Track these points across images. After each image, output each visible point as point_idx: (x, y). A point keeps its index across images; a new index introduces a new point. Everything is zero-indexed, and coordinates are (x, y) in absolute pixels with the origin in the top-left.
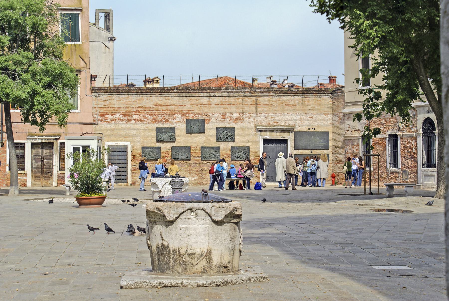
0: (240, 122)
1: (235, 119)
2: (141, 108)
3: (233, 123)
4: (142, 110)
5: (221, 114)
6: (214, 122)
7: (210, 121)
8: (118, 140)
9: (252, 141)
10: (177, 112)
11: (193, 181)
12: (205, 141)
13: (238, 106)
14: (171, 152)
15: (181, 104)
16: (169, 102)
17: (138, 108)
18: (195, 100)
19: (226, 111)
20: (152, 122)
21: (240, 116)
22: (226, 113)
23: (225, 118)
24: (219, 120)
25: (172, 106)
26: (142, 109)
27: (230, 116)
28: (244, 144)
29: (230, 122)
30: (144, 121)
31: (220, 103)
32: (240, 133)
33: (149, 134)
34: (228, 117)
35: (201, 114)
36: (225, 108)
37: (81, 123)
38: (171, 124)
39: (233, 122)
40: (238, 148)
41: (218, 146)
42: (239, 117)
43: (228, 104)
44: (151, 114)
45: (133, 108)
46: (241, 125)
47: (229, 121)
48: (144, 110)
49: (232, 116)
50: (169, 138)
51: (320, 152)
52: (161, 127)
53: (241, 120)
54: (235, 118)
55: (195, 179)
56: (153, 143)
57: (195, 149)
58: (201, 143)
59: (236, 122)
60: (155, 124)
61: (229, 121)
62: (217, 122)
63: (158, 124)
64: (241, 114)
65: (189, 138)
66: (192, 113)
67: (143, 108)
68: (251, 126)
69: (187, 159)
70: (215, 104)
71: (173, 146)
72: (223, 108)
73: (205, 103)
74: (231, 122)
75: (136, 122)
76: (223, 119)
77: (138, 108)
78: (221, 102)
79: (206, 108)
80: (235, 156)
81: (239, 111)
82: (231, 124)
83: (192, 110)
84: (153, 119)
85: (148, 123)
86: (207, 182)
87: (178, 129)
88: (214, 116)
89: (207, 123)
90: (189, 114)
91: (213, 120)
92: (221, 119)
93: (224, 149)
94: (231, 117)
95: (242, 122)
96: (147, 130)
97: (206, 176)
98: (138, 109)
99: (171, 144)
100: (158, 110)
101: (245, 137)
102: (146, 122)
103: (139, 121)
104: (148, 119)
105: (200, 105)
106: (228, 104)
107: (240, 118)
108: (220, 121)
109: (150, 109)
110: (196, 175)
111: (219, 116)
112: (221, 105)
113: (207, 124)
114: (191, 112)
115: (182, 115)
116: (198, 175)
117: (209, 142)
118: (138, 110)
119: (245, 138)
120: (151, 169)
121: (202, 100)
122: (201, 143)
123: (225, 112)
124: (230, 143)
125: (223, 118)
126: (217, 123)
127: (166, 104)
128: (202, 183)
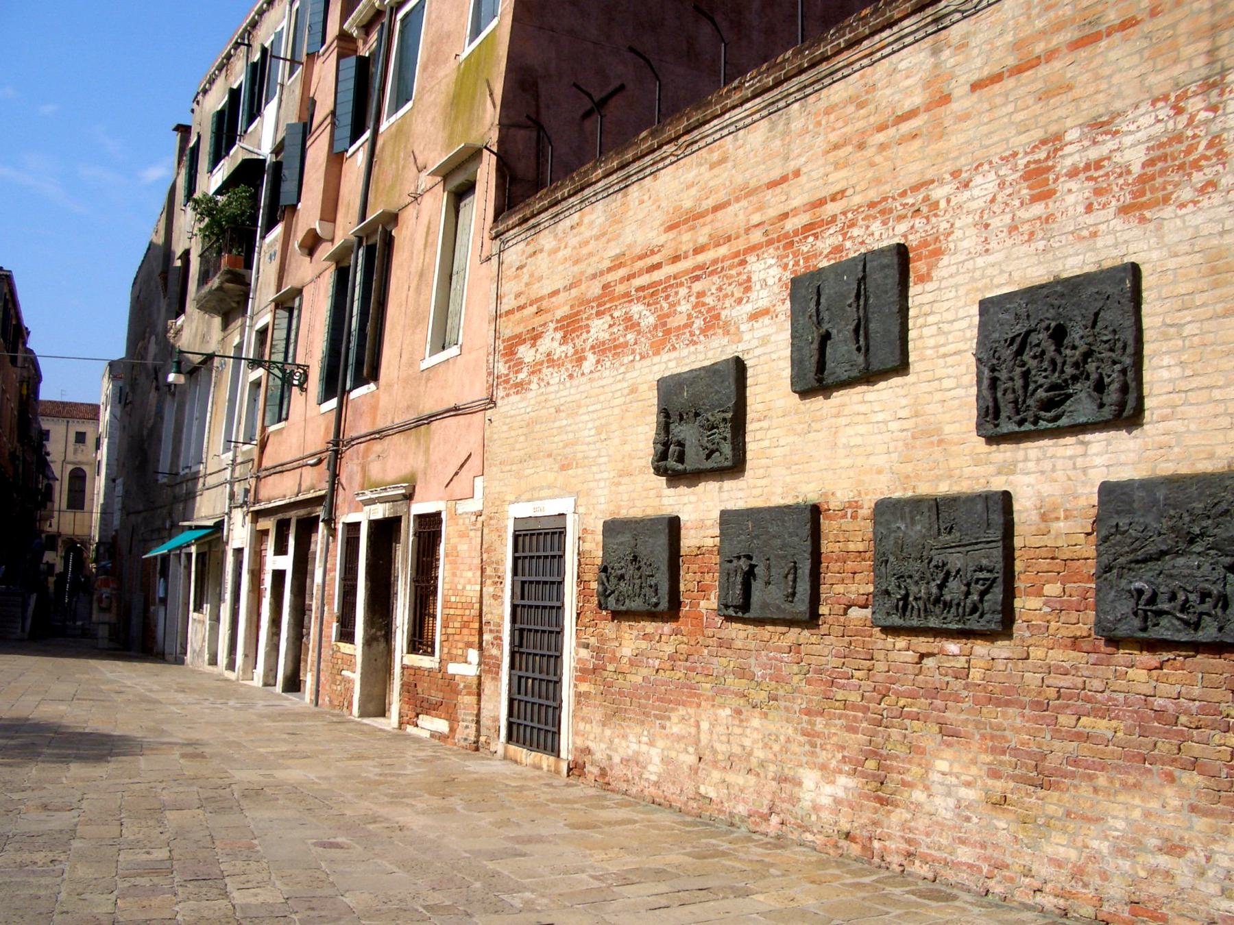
0: (1186, 194)
1: (1136, 169)
3: (1117, 224)
5: (1022, 162)
6: (971, 256)
7: (938, 253)
8: (541, 488)
10: (757, 237)
11: (826, 815)
12: (906, 445)
13: (1162, 21)
15: (776, 174)
16: (723, 180)
17: (610, 270)
18: (851, 109)
19: (1062, 112)
20: (651, 346)
21: (1183, 119)
22: (1055, 141)
23: (1049, 195)
24: (1007, 219)
25: (738, 200)
26: (622, 272)
27: (1094, 154)
29: (1090, 219)
31: (1011, 61)
32: (1187, 316)
33: (640, 429)
34: (1073, 173)
35: (882, 212)
36: (1043, 96)
37: (456, 409)
39: (1124, 210)
40: (1160, 495)
42: (1178, 138)
43: (1076, 45)
44: (650, 294)
46: (1199, 219)
49: (1112, 144)
51: (1016, 275)
53: (1196, 165)
54: (1135, 158)
55: (841, 794)
58: (879, 472)
60: (665, 356)
61: (1089, 209)
62: (993, 245)
64: (1195, 105)
66: (834, 219)
70: (975, 86)
72: (1030, 100)
73: (907, 105)
74: (1106, 218)
76: (1038, 209)
77: (610, 270)
78: (1017, 46)
79: (917, 143)
81: (1177, 70)
82: (1100, 243)
83: (833, 199)
86: (909, 841)
88: (967, 194)
89: (922, 279)
90: (816, 237)
91: (965, 239)
92: (1023, 214)
93: (1044, 517)
94: (1098, 165)
95: (1212, 184)
97: (904, 783)
98: (610, 277)
99: (725, 495)
104: (639, 333)
105: (881, 137)
106: (1076, 45)
107: (1188, 152)
108: (1013, 228)
111: (1002, 185)
112: (1018, 70)
114: (831, 208)
115: (781, 252)
117: (937, 453)
121: (888, 91)
122: (879, 472)
123: (1053, 128)
124: (1097, 440)
125: (1034, 199)
126: (990, 259)
127: (709, 203)
128: (876, 844)
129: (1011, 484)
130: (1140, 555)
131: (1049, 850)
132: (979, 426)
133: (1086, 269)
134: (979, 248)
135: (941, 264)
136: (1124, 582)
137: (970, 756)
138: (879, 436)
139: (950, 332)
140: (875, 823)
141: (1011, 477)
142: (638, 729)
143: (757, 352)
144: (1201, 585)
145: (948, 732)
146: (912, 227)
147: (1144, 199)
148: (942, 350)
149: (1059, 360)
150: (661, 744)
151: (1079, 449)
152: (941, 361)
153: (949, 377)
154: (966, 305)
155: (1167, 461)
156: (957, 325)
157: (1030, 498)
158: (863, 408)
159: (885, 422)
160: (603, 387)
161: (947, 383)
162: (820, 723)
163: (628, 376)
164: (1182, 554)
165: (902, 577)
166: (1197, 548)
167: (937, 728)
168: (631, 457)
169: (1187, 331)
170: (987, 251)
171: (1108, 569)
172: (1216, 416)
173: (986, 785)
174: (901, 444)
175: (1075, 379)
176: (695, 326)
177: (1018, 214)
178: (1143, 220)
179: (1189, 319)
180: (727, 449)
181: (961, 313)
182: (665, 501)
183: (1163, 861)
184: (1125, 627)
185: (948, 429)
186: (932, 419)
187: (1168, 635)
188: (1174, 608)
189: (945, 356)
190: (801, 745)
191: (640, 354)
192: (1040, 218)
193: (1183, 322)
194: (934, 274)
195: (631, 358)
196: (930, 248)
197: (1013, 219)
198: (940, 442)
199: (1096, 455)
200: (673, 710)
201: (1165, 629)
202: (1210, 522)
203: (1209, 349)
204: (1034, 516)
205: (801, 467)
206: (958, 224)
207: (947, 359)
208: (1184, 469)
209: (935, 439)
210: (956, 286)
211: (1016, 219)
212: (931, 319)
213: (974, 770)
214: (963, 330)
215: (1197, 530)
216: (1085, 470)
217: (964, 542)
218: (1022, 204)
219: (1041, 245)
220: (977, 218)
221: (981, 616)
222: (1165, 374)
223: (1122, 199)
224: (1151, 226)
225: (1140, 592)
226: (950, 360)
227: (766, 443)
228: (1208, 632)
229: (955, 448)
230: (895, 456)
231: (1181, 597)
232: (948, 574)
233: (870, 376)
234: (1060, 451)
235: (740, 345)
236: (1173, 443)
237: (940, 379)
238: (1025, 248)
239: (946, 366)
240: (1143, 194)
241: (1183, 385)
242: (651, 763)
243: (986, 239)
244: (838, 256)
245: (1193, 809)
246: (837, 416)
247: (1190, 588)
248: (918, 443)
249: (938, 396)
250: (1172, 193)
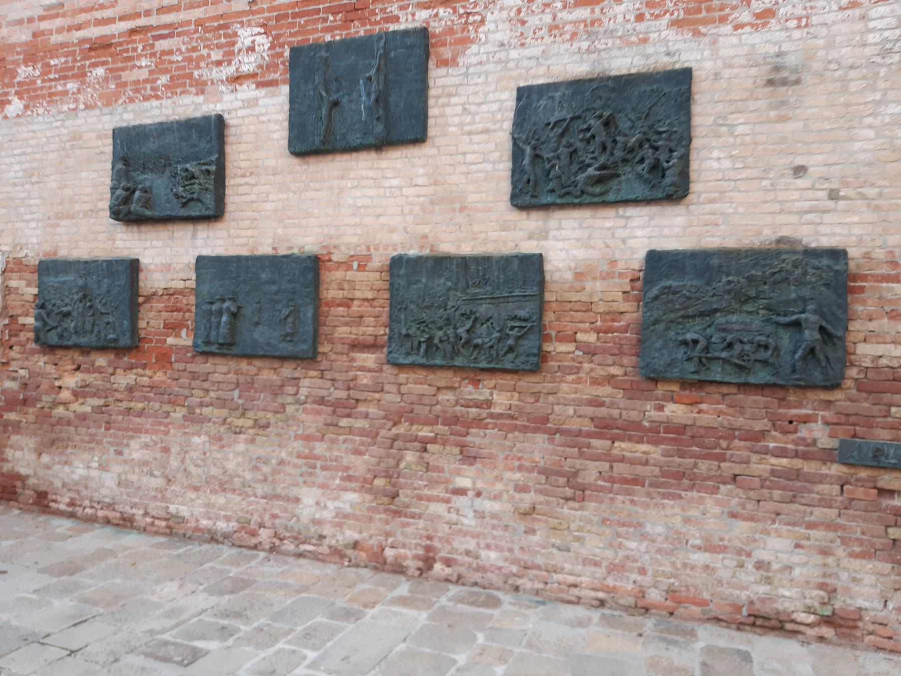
2: (57, 16)
3: (671, 34)
4: (60, 31)
7: (466, 42)
9: (871, 192)
12: (424, 210)
14: (192, 299)
17: (42, 18)
20: (101, 97)
24: (547, 18)
26: (59, 22)
28: (785, 232)
29: (641, 27)
30: (66, 93)
33: (84, 175)
38: (200, 99)
39: (676, 24)
41: (529, 247)
45: (20, 22)
47: (640, 18)
48: (70, 29)
50: (177, 196)
52: (148, 121)
56: (101, 237)
57: (350, 275)
58: (392, 231)
59: (705, 22)
61: (640, 18)
63: (131, 107)
65: (311, 194)
67: (64, 15)
68: (872, 38)
69: (286, 348)
71: (206, 252)
75: (26, 107)
77: (42, 18)
80: (685, 343)
82: (650, 50)
84: (106, 79)
85: (82, 106)
87: (244, 129)
89: (444, 63)
92: (564, 15)
96: (78, 152)
98: (44, 25)
99: (199, 242)
100: (138, 15)
101: (799, 161)
102: (76, 101)
103: (43, 97)
104: (83, 83)
108: (553, 28)
109: (98, 15)
110: (349, 478)
113: (442, 71)
116: (366, 485)
117: (460, 218)
118: (42, 33)
119: (800, 171)
120: (88, 409)
126: (526, 52)
129: (543, 247)
130: (690, 311)
131: (584, 552)
132: (513, 197)
133: (633, 71)
134: (513, 42)
135: (468, 52)
136: (671, 334)
137: (496, 473)
138: (392, 200)
139: (478, 113)
140: (388, 534)
141: (543, 243)
142: (86, 456)
143: (241, 113)
144: (758, 338)
145: (469, 457)
146: (436, 15)
147: (700, 16)
148: (467, 128)
149: (609, 145)
150: (116, 468)
151: (622, 222)
152: (466, 139)
153: (474, 153)
154: (496, 90)
155: (713, 236)
156: (484, 108)
157: (564, 260)
158: (371, 174)
159: (400, 188)
160: (34, 132)
161: (470, 158)
162: (320, 448)
163: (67, 123)
164: (733, 313)
165: (423, 322)
166: (749, 307)
167: (456, 450)
168: (72, 201)
169: (739, 130)
170: (523, 45)
171: (656, 322)
172: (765, 202)
173: (513, 498)
174: (417, 208)
175: (625, 161)
176: (159, 82)
177: (560, 15)
178: (696, 33)
179: (741, 121)
180: (209, 199)
181: (491, 97)
182: (119, 243)
183: (700, 558)
184: (676, 370)
185: (472, 198)
186: (454, 188)
187: (718, 378)
188: (732, 357)
189: (470, 133)
190: (296, 466)
191: (85, 104)
192: (584, 21)
193: (736, 122)
194: (461, 60)
195: (72, 106)
196: (457, 36)
197: (554, 19)
198: (462, 209)
199: (638, 227)
200: (132, 437)
201: (717, 373)
202: (766, 287)
203: (761, 147)
204: (569, 276)
205: (296, 221)
206: (489, 17)
207: (473, 137)
208: (731, 243)
209: (457, 206)
210: (487, 74)
211: (558, 20)
212: (454, 100)
213: (499, 486)
214: (493, 113)
215: (752, 293)
216: (624, 241)
217: (495, 296)
218: (565, 7)
219: (585, 45)
220: (512, 14)
221: (516, 357)
222: (715, 165)
223: (676, 14)
224: (706, 40)
225: (695, 342)
226: (476, 138)
227: (254, 197)
228: (763, 376)
229: (479, 215)
230: (410, 219)
231: (738, 348)
232: (476, 319)
233: (381, 145)
234: (598, 223)
235: (218, 105)
236: (720, 221)
237: (464, 154)
238: (567, 45)
239: (471, 142)
240: (699, 11)
241: (732, 175)
242: (103, 486)
243: (522, 34)
244: (344, 33)
245: (733, 515)
246: (342, 178)
247: (745, 340)
248: (437, 208)
249: (463, 168)
250: (729, 15)
